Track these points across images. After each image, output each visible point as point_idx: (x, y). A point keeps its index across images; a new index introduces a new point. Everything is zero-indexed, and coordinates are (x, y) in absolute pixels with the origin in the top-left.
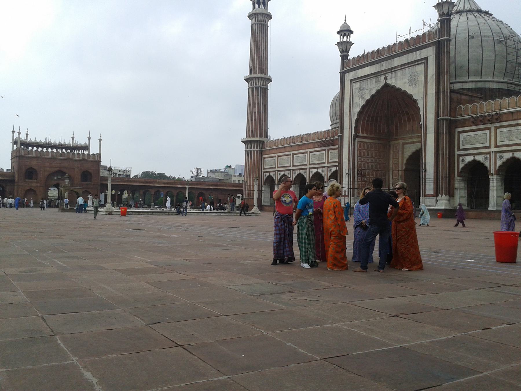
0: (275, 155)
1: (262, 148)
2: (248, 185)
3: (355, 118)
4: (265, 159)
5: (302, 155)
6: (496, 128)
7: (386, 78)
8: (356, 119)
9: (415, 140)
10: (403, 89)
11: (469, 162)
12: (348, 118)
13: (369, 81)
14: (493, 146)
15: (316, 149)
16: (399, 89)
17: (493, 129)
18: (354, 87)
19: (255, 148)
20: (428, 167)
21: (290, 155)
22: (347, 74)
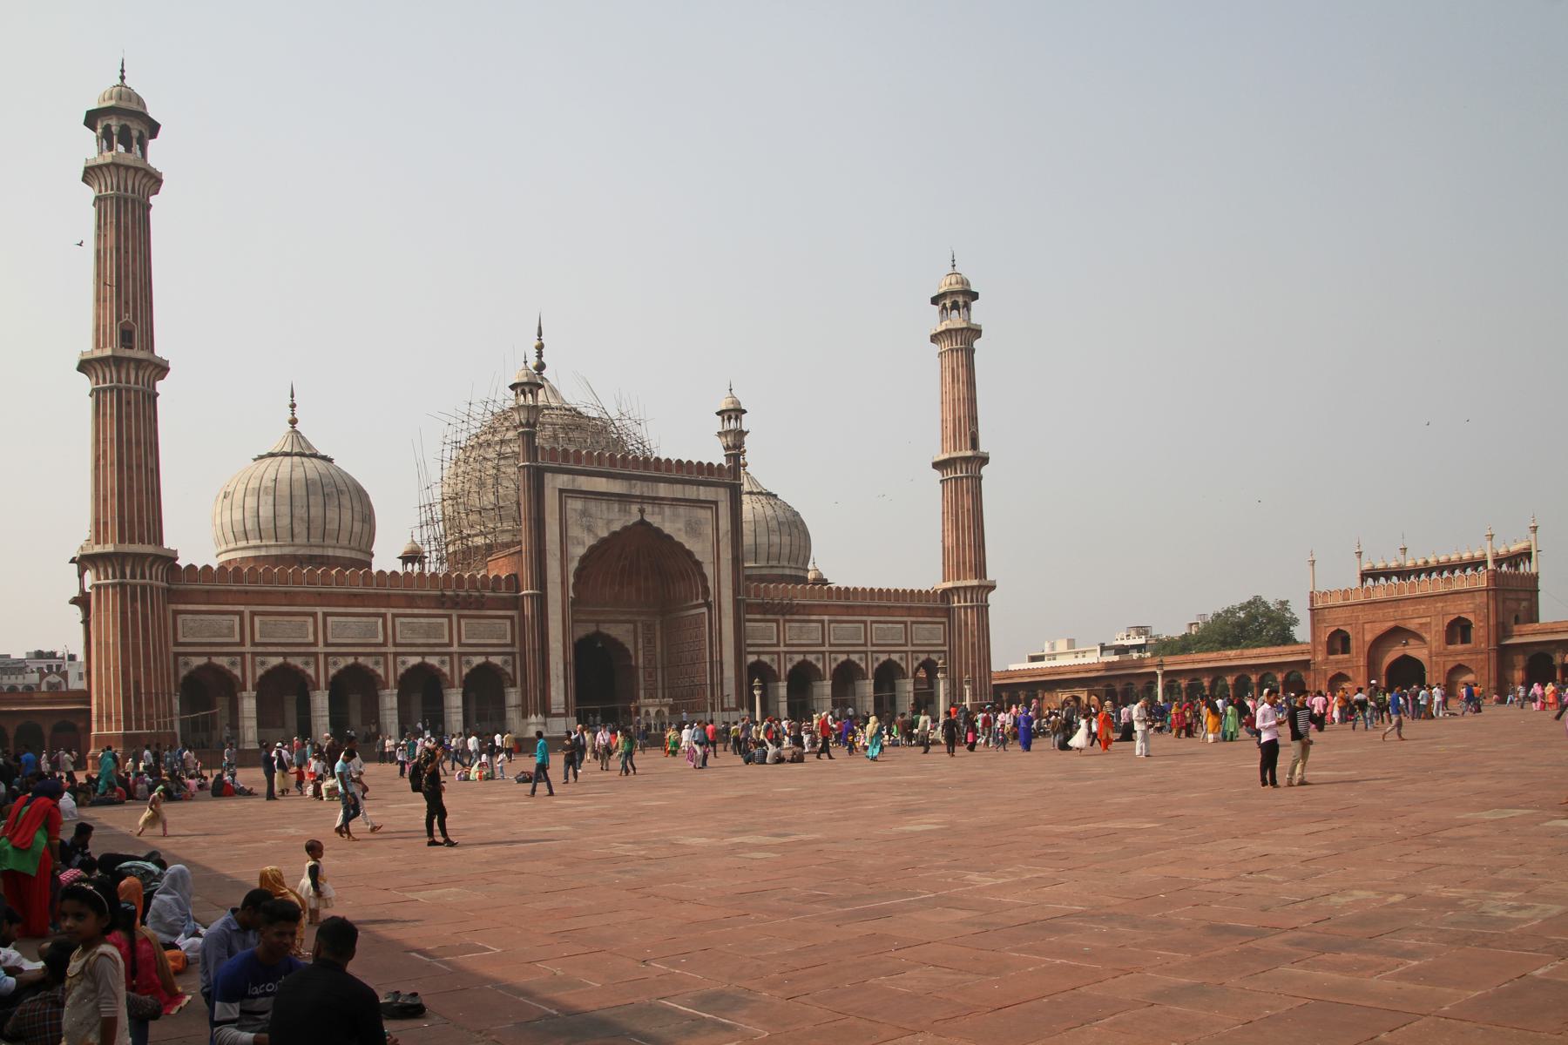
0: (241, 608)
1: (167, 582)
3: (574, 565)
4: (180, 618)
5: (364, 619)
6: (786, 621)
7: (642, 511)
10: (676, 539)
11: (753, 664)
12: (558, 562)
13: (604, 505)
15: (416, 611)
16: (669, 537)
18: (568, 506)
20: (725, 667)
21: (314, 615)
22: (550, 474)
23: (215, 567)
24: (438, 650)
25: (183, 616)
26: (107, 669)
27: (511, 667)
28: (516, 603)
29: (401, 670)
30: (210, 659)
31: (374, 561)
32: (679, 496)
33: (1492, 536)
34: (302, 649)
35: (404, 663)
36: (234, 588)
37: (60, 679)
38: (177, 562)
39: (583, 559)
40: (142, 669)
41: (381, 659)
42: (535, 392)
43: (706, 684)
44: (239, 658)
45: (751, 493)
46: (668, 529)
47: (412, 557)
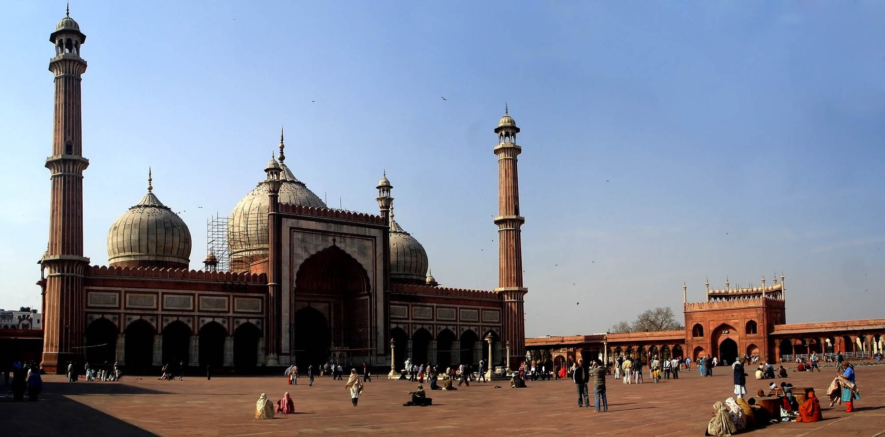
0: (120, 289)
2: (72, 332)
3: (296, 269)
4: (90, 293)
5: (183, 296)
6: (412, 306)
7: (334, 240)
8: (298, 271)
9: (301, 299)
10: (353, 257)
14: (410, 318)
15: (211, 293)
16: (349, 256)
17: (410, 306)
19: (79, 273)
20: (379, 331)
21: (157, 293)
23: (108, 267)
24: (221, 315)
25: (91, 293)
26: (53, 319)
27: (261, 326)
28: (265, 289)
29: (201, 325)
30: (103, 316)
31: (190, 264)
32: (356, 233)
33: (764, 281)
34: (150, 312)
35: (203, 321)
36: (117, 278)
37: (29, 322)
38: (89, 264)
39: (302, 266)
40: (69, 320)
41: (191, 319)
42: (278, 174)
43: (368, 340)
44: (117, 316)
45: (395, 232)
46: (348, 251)
47: (212, 261)
